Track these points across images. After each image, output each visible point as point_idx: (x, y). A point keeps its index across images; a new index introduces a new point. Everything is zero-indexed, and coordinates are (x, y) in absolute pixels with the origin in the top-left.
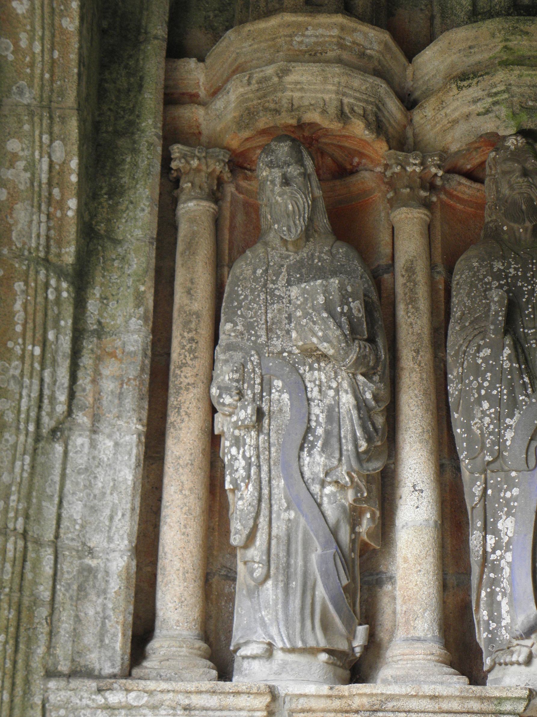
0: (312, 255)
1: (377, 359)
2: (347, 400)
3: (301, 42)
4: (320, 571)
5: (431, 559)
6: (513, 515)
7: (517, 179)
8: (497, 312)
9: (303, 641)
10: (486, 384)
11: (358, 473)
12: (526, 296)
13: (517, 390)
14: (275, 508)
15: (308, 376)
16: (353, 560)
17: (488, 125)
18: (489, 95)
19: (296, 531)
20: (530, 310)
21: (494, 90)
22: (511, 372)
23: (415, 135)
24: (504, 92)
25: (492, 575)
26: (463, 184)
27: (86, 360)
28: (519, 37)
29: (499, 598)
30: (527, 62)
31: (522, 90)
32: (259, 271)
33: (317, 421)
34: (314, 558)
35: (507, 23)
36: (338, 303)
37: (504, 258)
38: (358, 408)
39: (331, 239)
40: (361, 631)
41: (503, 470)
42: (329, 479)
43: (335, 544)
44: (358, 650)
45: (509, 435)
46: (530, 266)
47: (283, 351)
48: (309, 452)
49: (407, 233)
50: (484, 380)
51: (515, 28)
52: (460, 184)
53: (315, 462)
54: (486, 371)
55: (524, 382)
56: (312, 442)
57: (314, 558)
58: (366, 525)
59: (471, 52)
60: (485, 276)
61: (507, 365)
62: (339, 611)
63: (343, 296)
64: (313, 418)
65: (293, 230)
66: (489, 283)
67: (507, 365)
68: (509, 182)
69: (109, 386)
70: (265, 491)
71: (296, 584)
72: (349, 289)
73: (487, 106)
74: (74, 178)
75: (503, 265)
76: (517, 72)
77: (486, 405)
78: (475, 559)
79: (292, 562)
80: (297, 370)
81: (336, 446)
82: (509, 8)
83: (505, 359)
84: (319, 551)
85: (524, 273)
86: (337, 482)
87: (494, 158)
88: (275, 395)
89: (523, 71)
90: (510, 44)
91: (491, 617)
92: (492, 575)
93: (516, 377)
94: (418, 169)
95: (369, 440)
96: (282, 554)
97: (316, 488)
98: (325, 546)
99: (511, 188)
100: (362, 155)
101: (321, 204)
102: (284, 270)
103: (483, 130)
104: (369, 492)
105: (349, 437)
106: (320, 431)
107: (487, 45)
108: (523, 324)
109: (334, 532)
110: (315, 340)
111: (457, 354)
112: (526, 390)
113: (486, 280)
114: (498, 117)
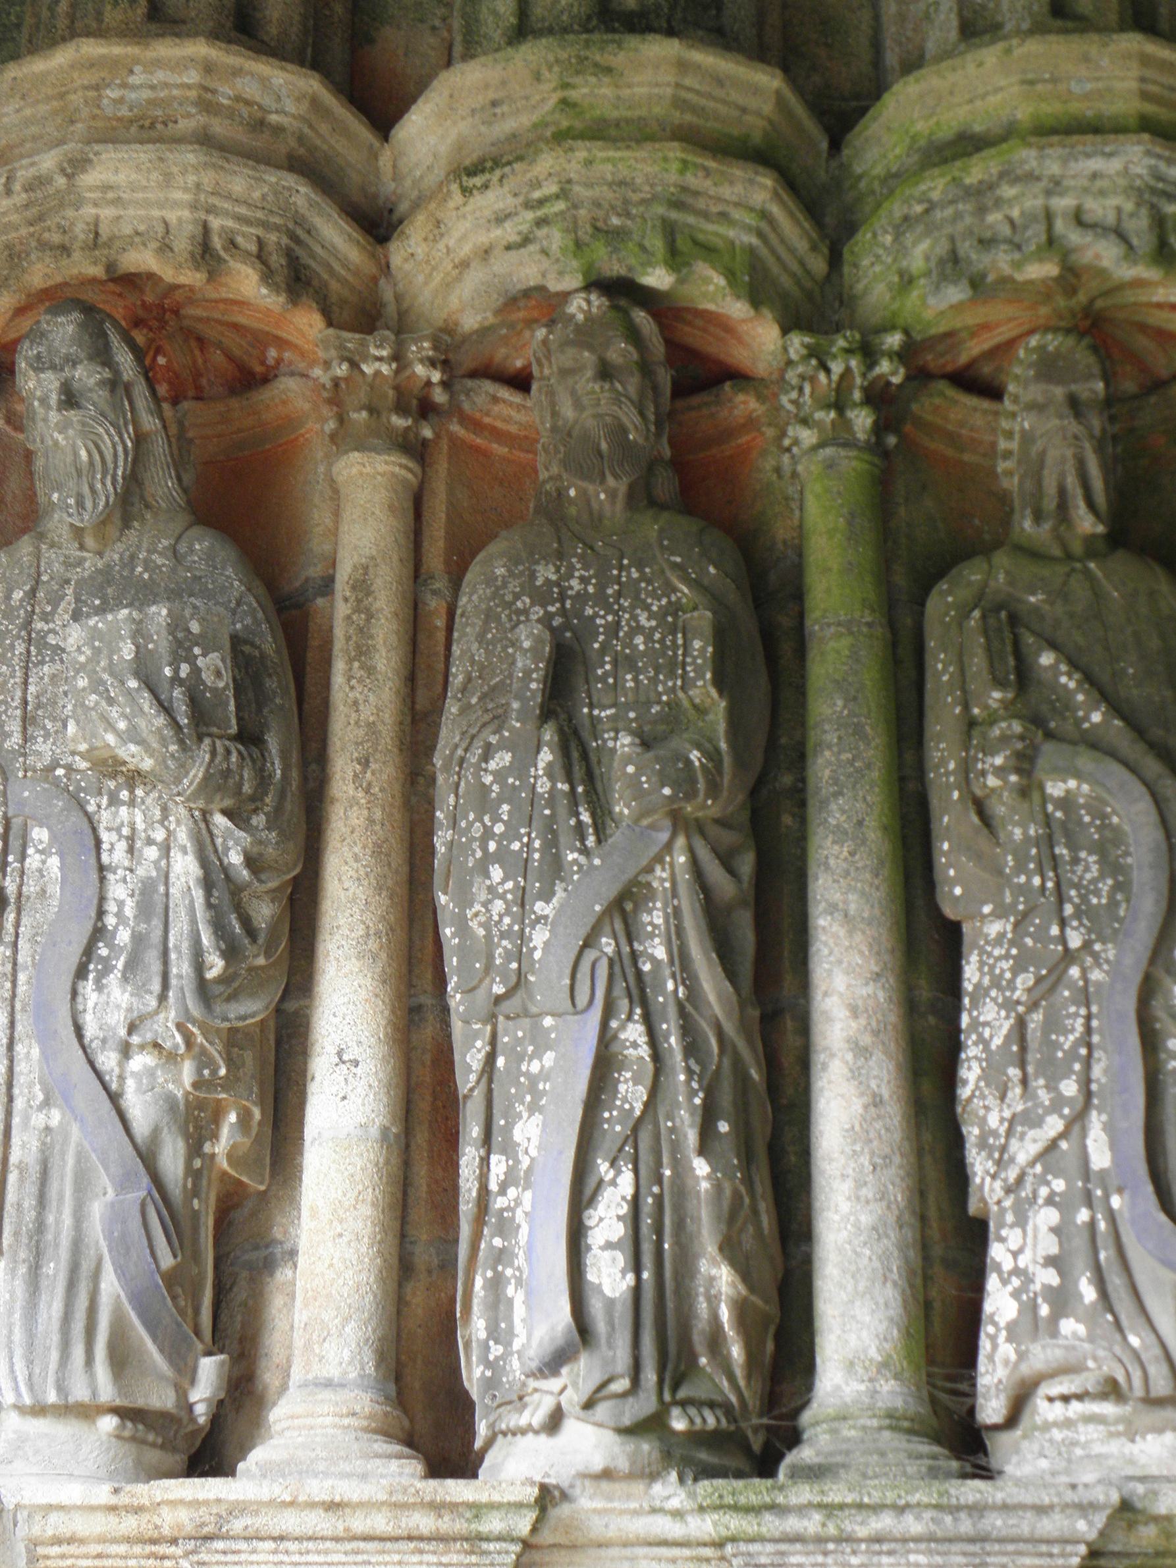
0: (133, 557)
1: (263, 779)
2: (185, 867)
3: (121, 100)
4: (109, 1236)
5: (367, 1210)
6: (541, 1110)
7: (586, 383)
8: (527, 673)
9: (61, 1388)
10: (499, 828)
11: (202, 1027)
12: (601, 638)
13: (563, 839)
14: (19, 1104)
15: (105, 816)
16: (195, 1215)
17: (528, 270)
18: (528, 205)
19: (63, 1153)
20: (608, 667)
21: (537, 195)
22: (551, 801)
23: (398, 298)
24: (557, 197)
25: (497, 1242)
26: (504, 401)
28: (593, 80)
29: (510, 1291)
30: (613, 132)
31: (596, 192)
32: (18, 595)
33: (119, 915)
34: (97, 1210)
35: (564, 48)
36: (166, 658)
37: (560, 555)
38: (208, 884)
39: (183, 519)
41: (526, 1013)
42: (135, 1040)
43: (146, 1180)
44: (200, 1409)
45: (539, 937)
46: (615, 572)
47: (55, 764)
48: (98, 981)
50: (496, 819)
51: (581, 60)
52: (495, 399)
53: (109, 1004)
54: (500, 800)
55: (580, 823)
56: (105, 961)
57: (97, 1210)
58: (226, 1140)
59: (495, 115)
60: (517, 597)
61: (543, 786)
62: (151, 1326)
63: (179, 643)
64: (111, 907)
65: (89, 504)
66: (526, 612)
67: (543, 786)
68: (573, 393)
71: (55, 1269)
72: (195, 627)
73: (524, 228)
75: (558, 570)
76: (581, 154)
77: (496, 873)
78: (466, 1207)
79: (50, 1219)
80: (82, 806)
81: (156, 967)
82: (589, 18)
83: (541, 772)
84: (111, 1193)
85: (601, 588)
86: (156, 1045)
87: (545, 342)
88: (33, 860)
89: (595, 151)
90: (573, 95)
91: (494, 1332)
92: (497, 1242)
93: (562, 811)
94: (385, 369)
95: (231, 953)
96: (29, 1203)
97: (108, 1060)
98: (122, 1186)
99: (578, 405)
100: (282, 343)
101: (159, 447)
102: (70, 591)
103: (519, 281)
104: (230, 1062)
105: (185, 946)
106: (124, 936)
107: (527, 98)
108: (590, 697)
109: (147, 1157)
110: (111, 738)
111: (447, 768)
112: (583, 839)
113: (519, 604)
114: (545, 252)
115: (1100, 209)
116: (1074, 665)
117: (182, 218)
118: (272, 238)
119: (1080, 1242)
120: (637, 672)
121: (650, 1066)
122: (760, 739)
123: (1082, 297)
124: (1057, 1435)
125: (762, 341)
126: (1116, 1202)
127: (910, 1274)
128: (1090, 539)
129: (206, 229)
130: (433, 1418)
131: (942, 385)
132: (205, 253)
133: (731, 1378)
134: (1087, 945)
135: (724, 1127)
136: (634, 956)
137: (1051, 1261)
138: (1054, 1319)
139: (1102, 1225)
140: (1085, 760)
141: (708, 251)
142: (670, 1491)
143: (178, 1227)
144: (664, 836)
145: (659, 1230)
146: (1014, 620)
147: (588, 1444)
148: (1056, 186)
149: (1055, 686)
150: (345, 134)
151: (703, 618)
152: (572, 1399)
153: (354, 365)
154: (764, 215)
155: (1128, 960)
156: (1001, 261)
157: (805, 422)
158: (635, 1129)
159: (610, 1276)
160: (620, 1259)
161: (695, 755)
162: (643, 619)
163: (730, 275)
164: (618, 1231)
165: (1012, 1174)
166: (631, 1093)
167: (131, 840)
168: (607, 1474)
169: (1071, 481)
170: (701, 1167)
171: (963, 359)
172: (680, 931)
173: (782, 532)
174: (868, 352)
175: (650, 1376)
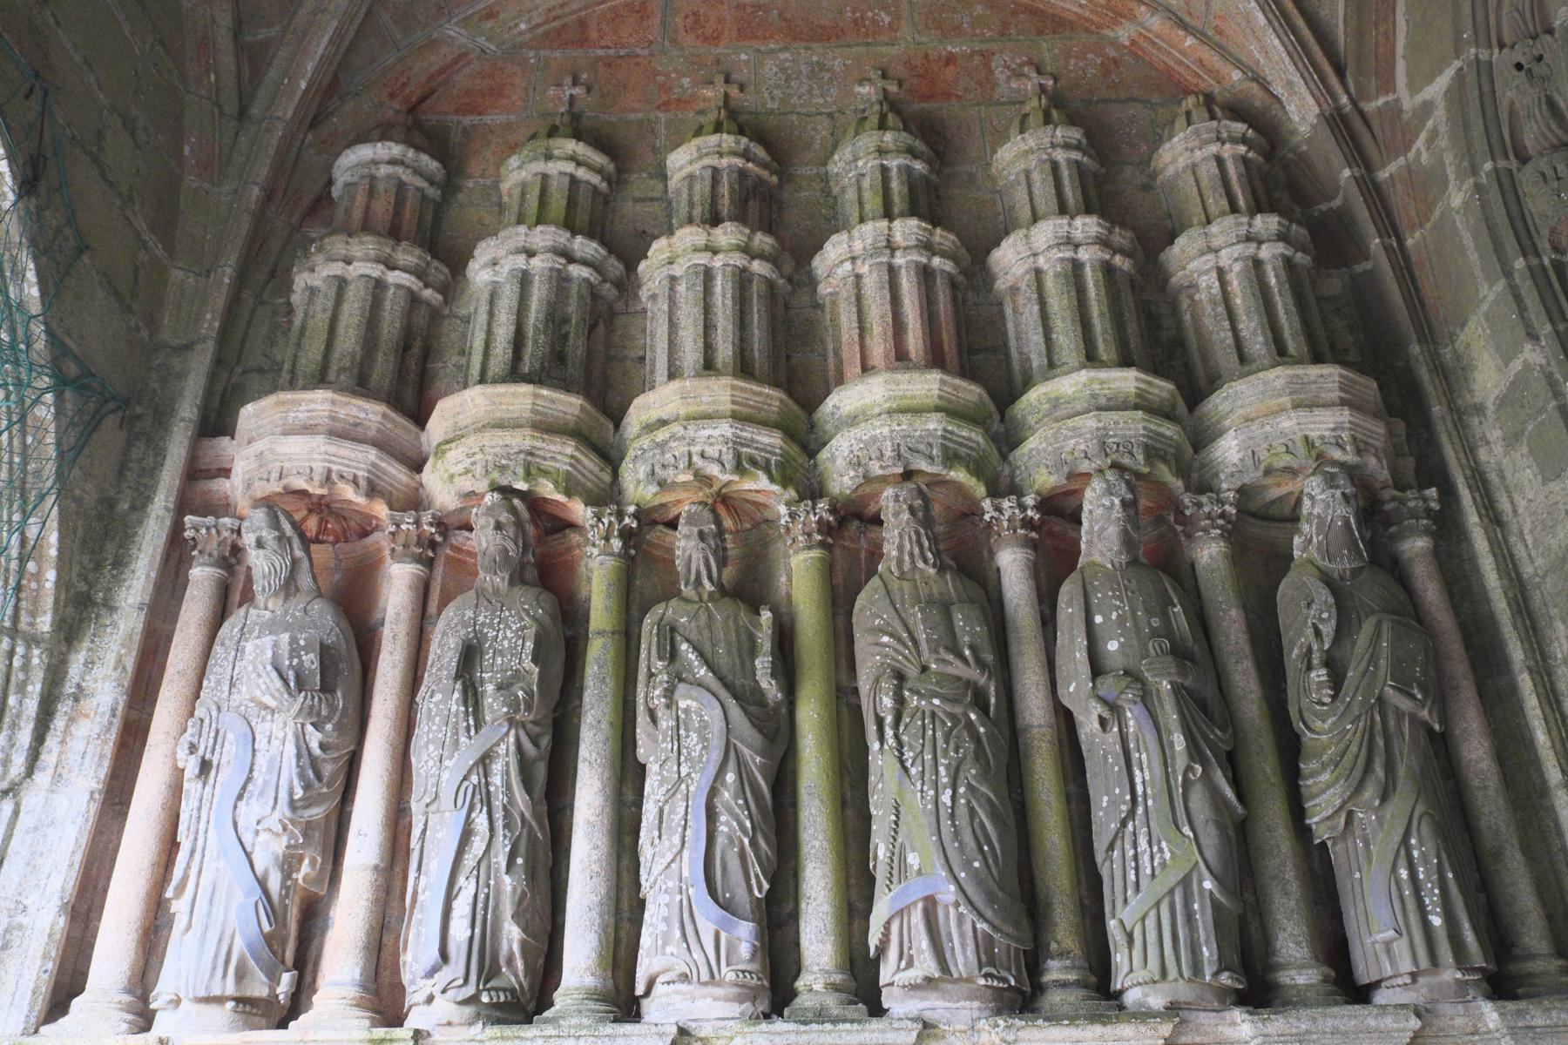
7: (490, 531)
9: (207, 988)
11: (292, 822)
17: (467, 484)
22: (456, 715)
27: (59, 723)
34: (234, 906)
36: (286, 655)
38: (299, 756)
40: (286, 978)
43: (259, 892)
44: (281, 997)
45: (445, 775)
49: (397, 585)
53: (250, 812)
63: (292, 650)
64: (256, 768)
69: (76, 745)
70: (200, 843)
72: (302, 643)
74: (53, 552)
81: (273, 794)
95: (307, 787)
97: (247, 838)
98: (248, 894)
109: (262, 883)
115: (712, 451)
116: (694, 648)
117: (319, 467)
118: (360, 473)
119: (676, 910)
120: (503, 656)
121: (488, 834)
122: (557, 685)
123: (715, 488)
124: (664, 1000)
125: (580, 511)
126: (691, 891)
127: (604, 928)
128: (711, 594)
129: (329, 471)
130: (384, 999)
131: (661, 527)
132: (328, 479)
133: (516, 976)
134: (688, 774)
135: (520, 861)
136: (487, 784)
137: (666, 920)
138: (664, 946)
139: (685, 903)
140: (695, 691)
141: (545, 473)
143: (275, 912)
144: (505, 729)
145: (486, 909)
146: (673, 630)
147: (445, 1007)
148: (693, 441)
149: (687, 659)
150: (400, 426)
151: (531, 632)
152: (436, 991)
153: (398, 526)
154: (572, 457)
156: (670, 474)
157: (594, 545)
158: (479, 863)
159: (460, 930)
160: (466, 923)
161: (520, 693)
162: (509, 634)
163: (556, 483)
164: (467, 910)
165: (652, 880)
166: (478, 846)
168: (449, 1024)
169: (702, 567)
170: (507, 880)
171: (671, 516)
172: (508, 773)
173: (584, 593)
174: (620, 515)
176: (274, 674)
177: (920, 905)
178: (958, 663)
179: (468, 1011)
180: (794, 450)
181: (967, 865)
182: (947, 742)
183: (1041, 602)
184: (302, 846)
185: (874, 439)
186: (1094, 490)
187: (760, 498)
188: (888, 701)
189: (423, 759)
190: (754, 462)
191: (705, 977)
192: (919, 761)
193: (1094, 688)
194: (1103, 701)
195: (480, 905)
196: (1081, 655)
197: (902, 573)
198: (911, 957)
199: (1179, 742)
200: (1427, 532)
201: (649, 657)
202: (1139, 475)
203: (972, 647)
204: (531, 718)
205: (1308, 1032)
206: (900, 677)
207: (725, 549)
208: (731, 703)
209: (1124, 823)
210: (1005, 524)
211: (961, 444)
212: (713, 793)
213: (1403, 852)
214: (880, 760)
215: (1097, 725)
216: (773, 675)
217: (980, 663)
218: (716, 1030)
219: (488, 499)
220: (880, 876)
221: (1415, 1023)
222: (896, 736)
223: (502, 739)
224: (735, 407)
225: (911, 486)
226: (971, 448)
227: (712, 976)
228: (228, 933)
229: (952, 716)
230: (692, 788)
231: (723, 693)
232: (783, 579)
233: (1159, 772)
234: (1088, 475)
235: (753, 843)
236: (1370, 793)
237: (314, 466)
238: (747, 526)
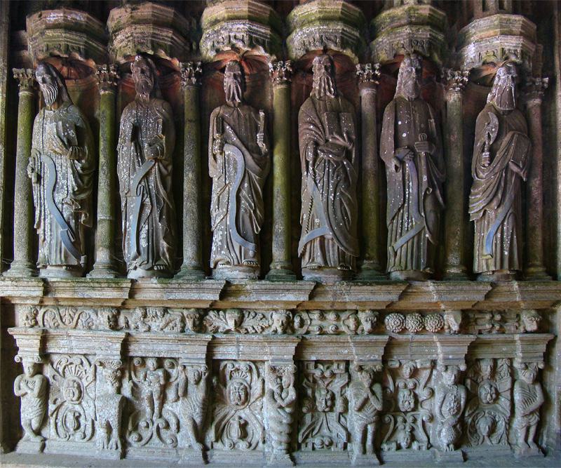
36: (62, 130)
38: (73, 173)
45: (132, 182)
53: (59, 197)
62: (71, 251)
63: (64, 129)
95: (78, 186)
97: (60, 206)
109: (68, 223)
115: (239, 35)
119: (225, 237)
123: (241, 54)
132: (67, 49)
133: (167, 260)
134: (229, 183)
136: (148, 186)
137: (221, 241)
140: (232, 147)
142: (154, 280)
143: (75, 234)
144: (153, 163)
146: (223, 119)
148: (231, 31)
152: (137, 265)
155: (235, 186)
159: (143, 244)
166: (148, 211)
167: (61, 166)
168: (143, 277)
169: (235, 92)
171: (222, 66)
175: (151, 261)
176: (58, 139)
177: (318, 239)
178: (342, 140)
179: (150, 272)
180: (276, 36)
181: (338, 225)
182: (334, 173)
183: (377, 114)
184: (81, 209)
185: (311, 32)
186: (405, 63)
187: (262, 60)
188: (310, 154)
189: (123, 175)
190: (257, 40)
191: (236, 263)
192: (322, 181)
193: (395, 153)
194: (397, 158)
195: (150, 235)
196: (391, 139)
197: (320, 97)
198: (314, 258)
199: (425, 178)
200: (541, 97)
201: (213, 133)
202: (424, 57)
203: (347, 133)
204: (164, 158)
205: (452, 290)
206: (316, 144)
207: (245, 83)
208: (247, 153)
209: (399, 210)
210: (365, 76)
211: (350, 37)
212: (239, 191)
213: (500, 227)
214: (307, 180)
215: (394, 169)
216: (264, 142)
217: (350, 139)
218: (240, 282)
219: (137, 58)
220: (304, 226)
221: (490, 288)
222: (313, 169)
223: (153, 167)
224: (250, 14)
225: (325, 57)
226: (353, 39)
227: (239, 263)
228: (59, 241)
229: (337, 163)
230: (231, 189)
231: (244, 149)
232: (270, 97)
233: (415, 191)
234: (403, 56)
235: (255, 211)
236: (494, 204)
237: (61, 43)
238: (255, 72)
